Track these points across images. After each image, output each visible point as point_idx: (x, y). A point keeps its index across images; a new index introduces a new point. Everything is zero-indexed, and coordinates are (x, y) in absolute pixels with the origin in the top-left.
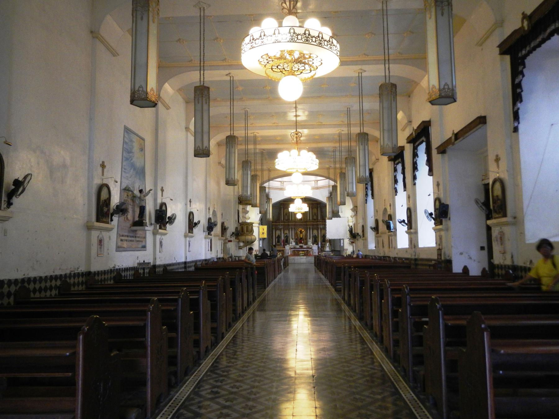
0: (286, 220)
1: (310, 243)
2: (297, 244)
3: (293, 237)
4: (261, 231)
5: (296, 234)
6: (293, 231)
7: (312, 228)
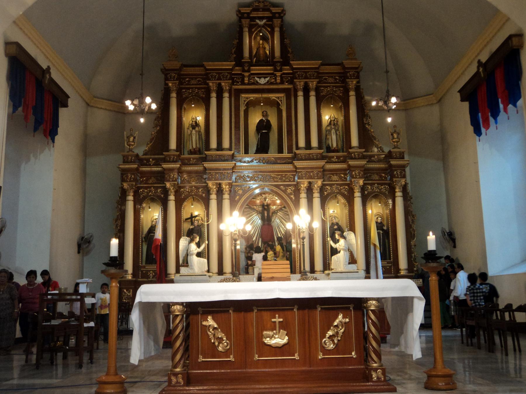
7: (322, 190)
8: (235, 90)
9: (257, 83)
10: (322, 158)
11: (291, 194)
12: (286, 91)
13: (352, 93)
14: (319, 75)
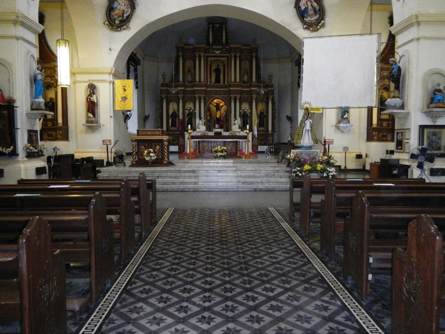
0: (189, 82)
1: (235, 128)
2: (209, 129)
3: (202, 116)
4: (119, 93)
5: (208, 110)
6: (202, 104)
7: (240, 99)
8: (206, 56)
9: (215, 53)
10: (241, 86)
11: (228, 100)
12: (227, 57)
13: (254, 59)
14: (241, 51)
